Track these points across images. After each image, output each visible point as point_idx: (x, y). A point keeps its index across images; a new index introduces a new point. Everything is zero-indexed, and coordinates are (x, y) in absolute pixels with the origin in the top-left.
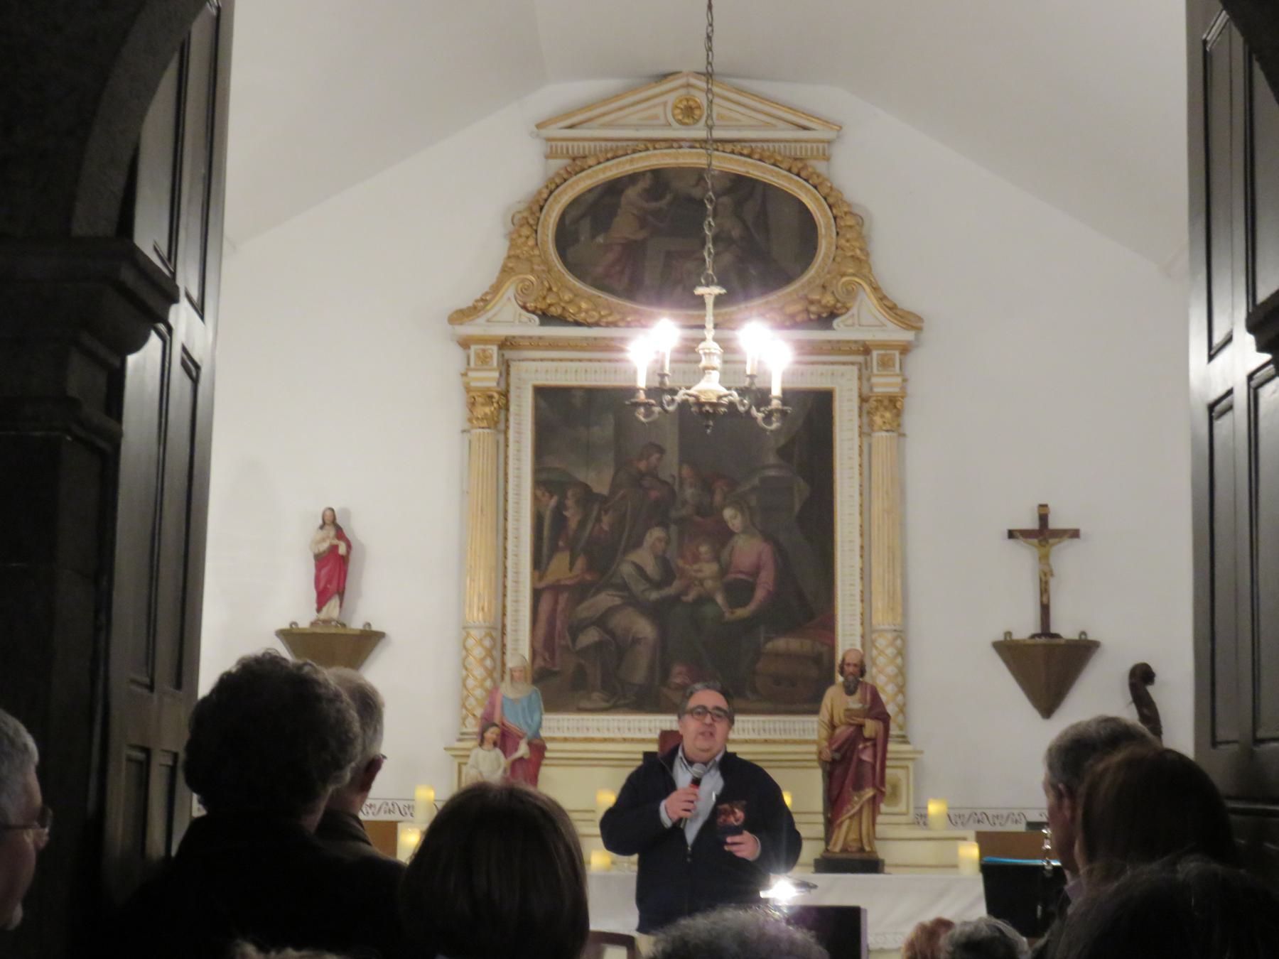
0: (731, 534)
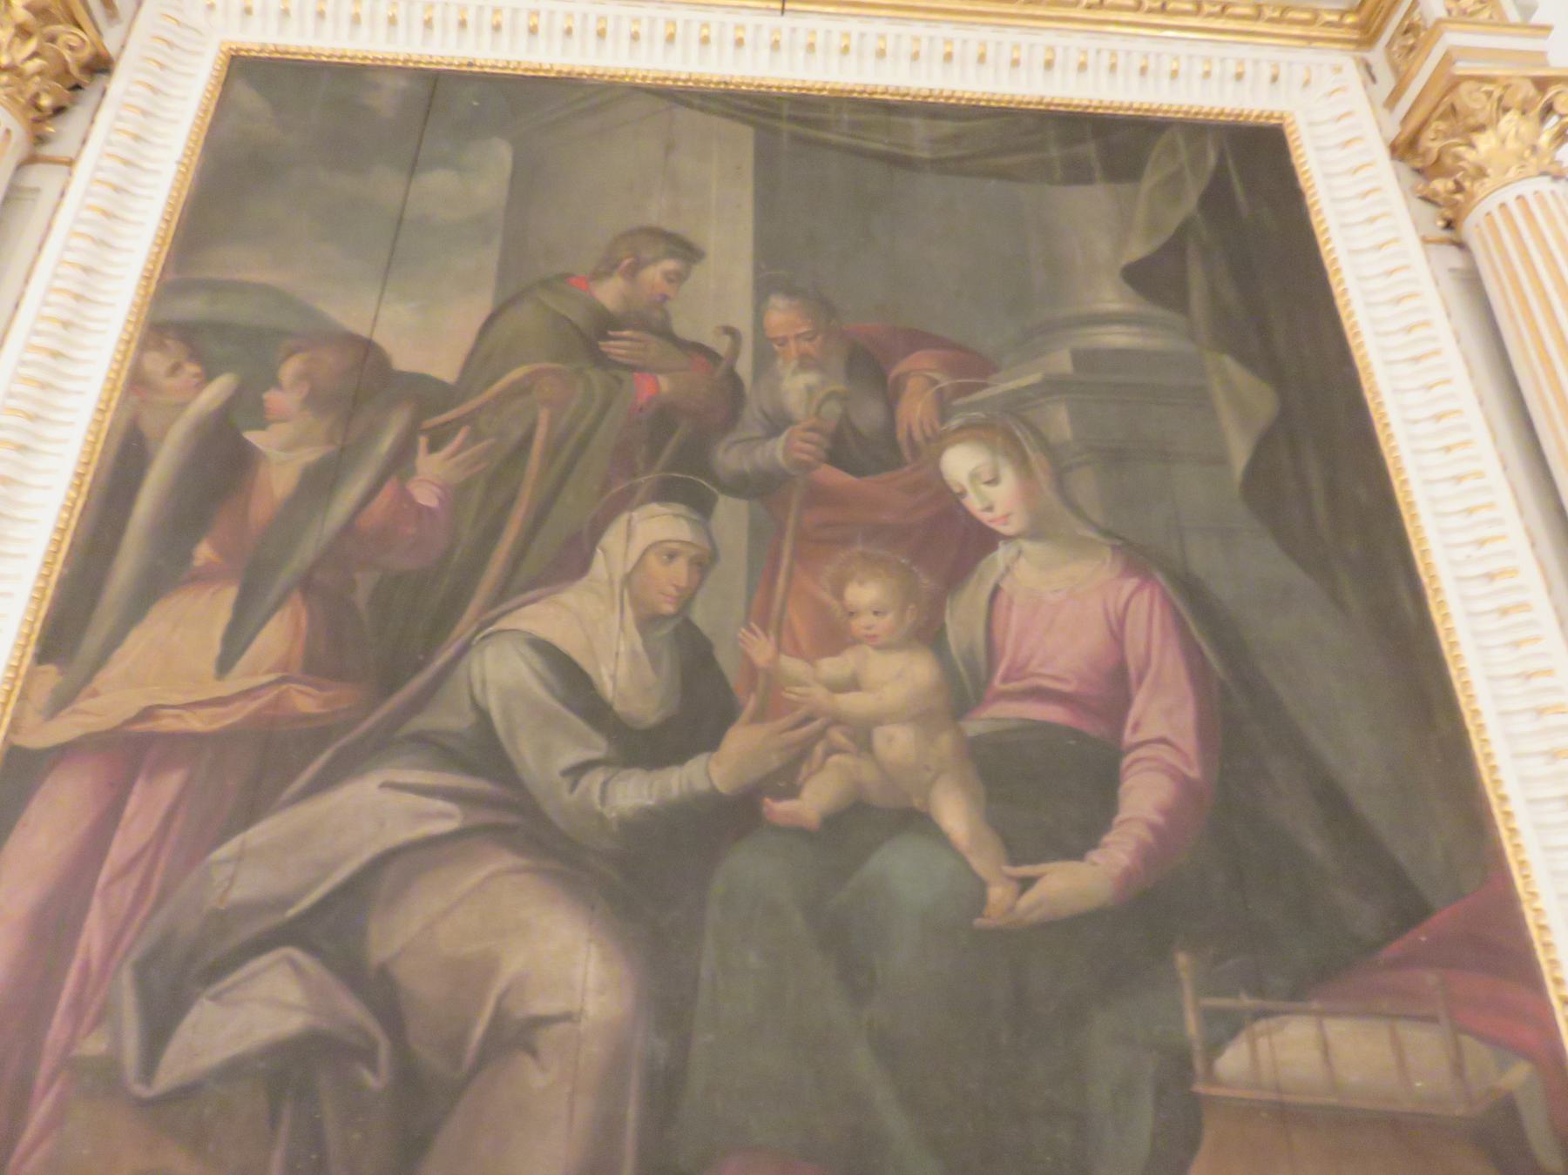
0: (984, 539)
